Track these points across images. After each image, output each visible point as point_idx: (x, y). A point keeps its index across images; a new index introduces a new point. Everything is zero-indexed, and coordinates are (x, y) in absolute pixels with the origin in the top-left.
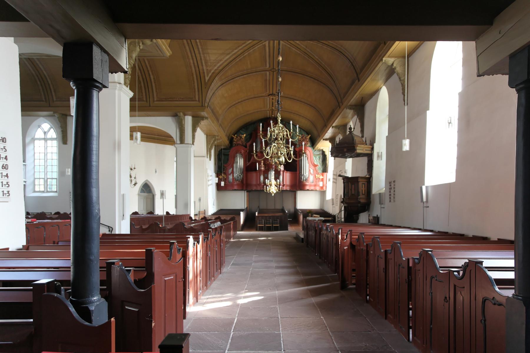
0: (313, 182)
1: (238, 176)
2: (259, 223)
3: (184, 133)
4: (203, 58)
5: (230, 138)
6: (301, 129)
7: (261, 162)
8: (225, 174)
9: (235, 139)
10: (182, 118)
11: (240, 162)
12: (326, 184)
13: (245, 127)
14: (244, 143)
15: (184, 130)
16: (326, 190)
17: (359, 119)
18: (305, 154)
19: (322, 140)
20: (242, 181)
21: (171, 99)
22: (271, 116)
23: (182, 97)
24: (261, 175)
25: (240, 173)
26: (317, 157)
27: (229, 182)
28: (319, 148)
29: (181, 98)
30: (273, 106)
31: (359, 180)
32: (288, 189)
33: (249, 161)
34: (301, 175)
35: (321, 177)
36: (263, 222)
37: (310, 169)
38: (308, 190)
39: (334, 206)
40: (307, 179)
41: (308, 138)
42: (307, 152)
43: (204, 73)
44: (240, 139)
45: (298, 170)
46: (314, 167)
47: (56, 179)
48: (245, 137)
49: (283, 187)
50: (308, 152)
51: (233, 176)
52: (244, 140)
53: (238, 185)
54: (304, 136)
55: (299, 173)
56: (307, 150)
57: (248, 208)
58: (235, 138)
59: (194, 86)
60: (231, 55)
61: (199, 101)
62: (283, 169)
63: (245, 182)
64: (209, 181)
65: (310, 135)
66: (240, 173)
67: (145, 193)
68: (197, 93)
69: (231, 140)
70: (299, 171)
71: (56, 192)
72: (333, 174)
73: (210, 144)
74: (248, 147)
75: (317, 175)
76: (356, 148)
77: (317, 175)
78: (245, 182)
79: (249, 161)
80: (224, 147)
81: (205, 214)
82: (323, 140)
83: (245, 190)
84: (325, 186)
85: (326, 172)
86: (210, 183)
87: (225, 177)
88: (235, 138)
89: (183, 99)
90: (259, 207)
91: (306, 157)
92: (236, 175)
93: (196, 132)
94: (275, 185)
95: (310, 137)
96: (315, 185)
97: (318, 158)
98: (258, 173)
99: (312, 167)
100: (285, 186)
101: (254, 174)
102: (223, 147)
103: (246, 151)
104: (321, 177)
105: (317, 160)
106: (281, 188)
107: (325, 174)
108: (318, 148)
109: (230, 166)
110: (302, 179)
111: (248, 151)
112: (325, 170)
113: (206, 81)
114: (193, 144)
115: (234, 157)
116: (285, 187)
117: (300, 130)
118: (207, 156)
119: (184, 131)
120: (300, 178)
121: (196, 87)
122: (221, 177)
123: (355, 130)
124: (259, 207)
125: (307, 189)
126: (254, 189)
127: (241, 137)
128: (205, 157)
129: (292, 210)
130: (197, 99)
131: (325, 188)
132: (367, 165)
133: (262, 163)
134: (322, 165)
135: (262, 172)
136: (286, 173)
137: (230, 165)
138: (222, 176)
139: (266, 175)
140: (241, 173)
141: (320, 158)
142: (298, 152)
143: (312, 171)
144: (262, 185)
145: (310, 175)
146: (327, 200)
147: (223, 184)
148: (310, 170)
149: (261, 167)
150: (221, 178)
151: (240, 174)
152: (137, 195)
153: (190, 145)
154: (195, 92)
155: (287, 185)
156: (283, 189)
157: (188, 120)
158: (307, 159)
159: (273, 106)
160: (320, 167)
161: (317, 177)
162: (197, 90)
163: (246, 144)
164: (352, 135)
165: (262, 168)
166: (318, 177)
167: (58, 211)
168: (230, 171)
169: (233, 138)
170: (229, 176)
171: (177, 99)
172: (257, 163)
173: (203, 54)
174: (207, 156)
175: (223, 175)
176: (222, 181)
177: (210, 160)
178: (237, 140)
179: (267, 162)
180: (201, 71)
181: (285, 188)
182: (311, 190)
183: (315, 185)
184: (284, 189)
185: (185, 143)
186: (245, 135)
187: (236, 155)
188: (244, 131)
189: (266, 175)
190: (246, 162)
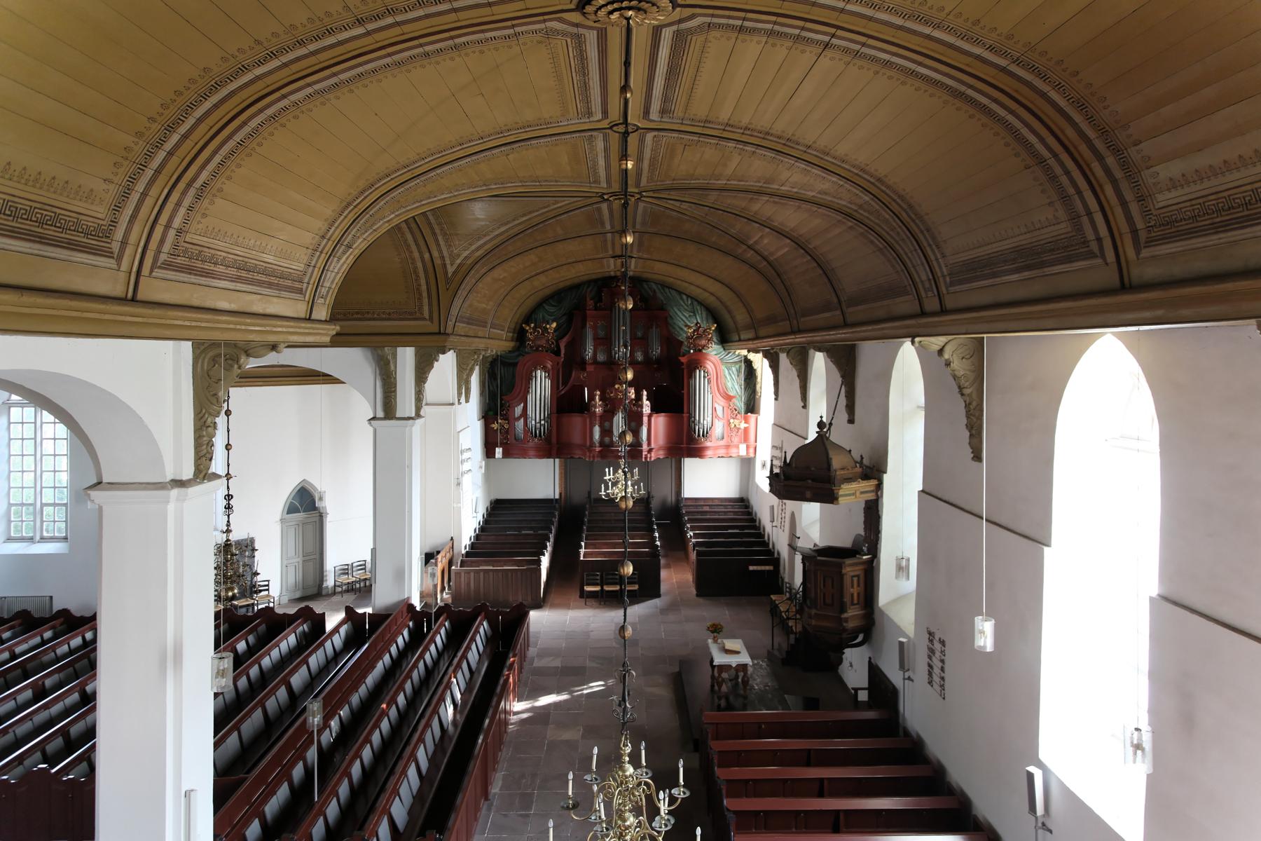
1: (538, 425)
2: (587, 579)
3: (395, 391)
4: (438, 231)
6: (693, 301)
7: (596, 395)
8: (505, 418)
9: (531, 335)
10: (390, 357)
11: (541, 387)
12: (756, 442)
13: (558, 296)
14: (553, 343)
15: (396, 384)
16: (755, 457)
17: (845, 386)
20: (548, 439)
21: (359, 316)
23: (387, 311)
24: (595, 426)
25: (542, 418)
26: (734, 369)
27: (515, 438)
29: (384, 313)
31: (844, 571)
32: (661, 457)
34: (694, 422)
35: (743, 425)
36: (599, 578)
37: (716, 405)
39: (774, 524)
42: (708, 366)
43: (443, 258)
44: (543, 334)
45: (685, 410)
46: (724, 401)
47: (65, 505)
48: (556, 330)
49: (649, 456)
50: (709, 366)
54: (700, 327)
55: (689, 418)
56: (708, 362)
59: (419, 285)
60: (511, 225)
61: (431, 319)
62: (649, 411)
63: (554, 440)
64: (462, 462)
67: (300, 512)
68: (425, 301)
69: (520, 336)
70: (689, 412)
71: (66, 538)
72: (773, 447)
73: (466, 369)
74: (563, 351)
75: (732, 421)
76: (838, 493)
77: (732, 421)
78: (554, 440)
79: (565, 384)
81: (453, 548)
84: (754, 446)
86: (466, 467)
89: (389, 314)
90: (589, 493)
91: (704, 377)
92: (533, 422)
93: (425, 383)
95: (716, 328)
96: (728, 447)
97: (735, 372)
100: (654, 450)
101: (576, 421)
104: (743, 425)
105: (733, 376)
106: (644, 456)
107: (752, 417)
109: (518, 398)
110: (695, 433)
112: (752, 406)
113: (450, 275)
114: (418, 415)
115: (529, 378)
116: (653, 454)
117: (692, 303)
118: (459, 400)
119: (395, 387)
120: (691, 430)
121: (424, 287)
122: (495, 426)
123: (832, 428)
124: (589, 493)
128: (453, 404)
129: (671, 499)
130: (426, 314)
132: (863, 511)
133: (597, 397)
134: (745, 389)
135: (598, 418)
137: (518, 395)
139: (607, 424)
140: (544, 419)
141: (739, 371)
142: (685, 364)
144: (598, 449)
145: (716, 421)
147: (499, 452)
148: (714, 409)
150: (495, 428)
151: (543, 422)
152: (279, 523)
153: (411, 421)
154: (420, 299)
156: (648, 460)
157: (406, 357)
158: (709, 383)
160: (740, 404)
161: (733, 426)
162: (425, 294)
163: (558, 346)
164: (824, 444)
166: (735, 425)
167: (66, 607)
168: (518, 410)
170: (516, 424)
171: (375, 316)
172: (586, 389)
173: (439, 224)
174: (459, 400)
175: (499, 421)
177: (467, 401)
178: (536, 338)
180: (438, 262)
181: (653, 456)
183: (728, 447)
184: (650, 458)
185: (398, 415)
186: (554, 325)
187: (534, 374)
188: (553, 306)
189: (607, 424)
190: (558, 388)
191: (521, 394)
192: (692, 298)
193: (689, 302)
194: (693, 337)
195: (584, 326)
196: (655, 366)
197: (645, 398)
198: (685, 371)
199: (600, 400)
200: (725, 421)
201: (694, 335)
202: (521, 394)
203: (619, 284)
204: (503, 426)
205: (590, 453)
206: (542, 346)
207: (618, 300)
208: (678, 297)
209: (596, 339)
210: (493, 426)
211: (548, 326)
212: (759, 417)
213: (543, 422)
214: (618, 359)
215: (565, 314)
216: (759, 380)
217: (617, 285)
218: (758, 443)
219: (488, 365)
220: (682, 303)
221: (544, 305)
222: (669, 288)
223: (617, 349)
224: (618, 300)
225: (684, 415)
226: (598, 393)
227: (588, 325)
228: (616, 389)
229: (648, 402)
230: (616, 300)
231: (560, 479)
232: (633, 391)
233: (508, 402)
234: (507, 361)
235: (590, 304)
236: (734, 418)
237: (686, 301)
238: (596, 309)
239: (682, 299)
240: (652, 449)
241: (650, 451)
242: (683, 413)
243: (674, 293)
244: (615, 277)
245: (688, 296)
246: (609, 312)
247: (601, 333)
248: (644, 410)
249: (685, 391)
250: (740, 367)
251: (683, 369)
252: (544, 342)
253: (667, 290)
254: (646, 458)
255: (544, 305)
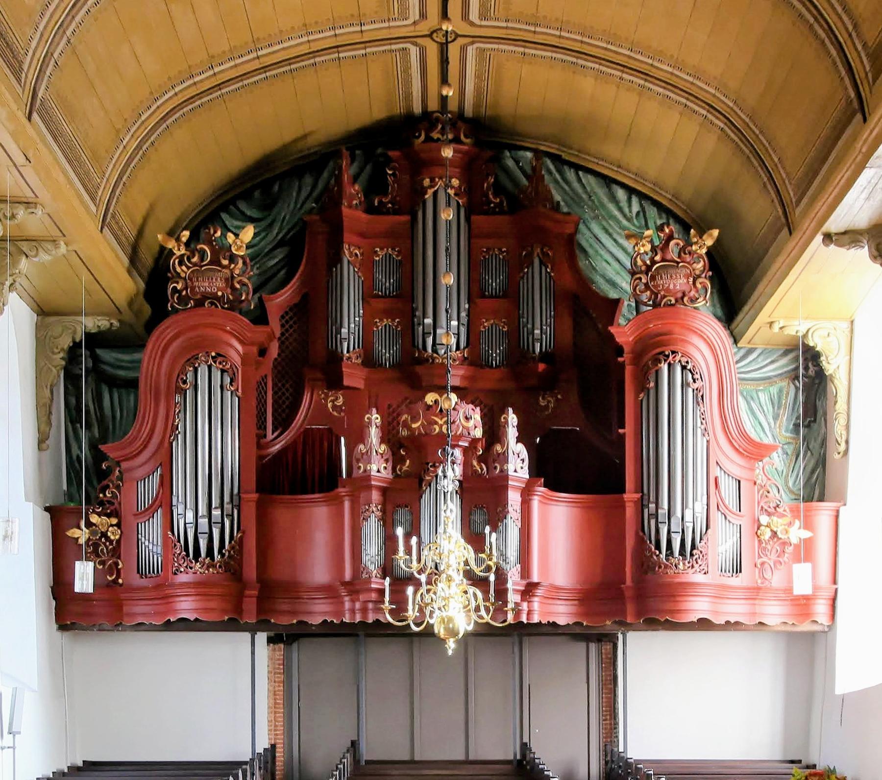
0: (738, 570)
5: (147, 258)
6: (647, 205)
12: (835, 581)
14: (243, 284)
18: (684, 368)
19: (819, 238)
22: (433, 105)
25: (215, 502)
26: (763, 397)
28: (776, 328)
30: (444, 80)
32: (562, 621)
33: (283, 423)
35: (797, 534)
37: (716, 472)
38: (704, 624)
40: (693, 547)
41: (704, 251)
44: (215, 261)
49: (525, 605)
51: (169, 524)
52: (243, 273)
53: (200, 587)
55: (641, 505)
57: (279, 754)
58: (183, 251)
62: (524, 474)
63: (250, 572)
65: (716, 233)
66: (215, 502)
70: (640, 488)
75: (764, 519)
77: (764, 519)
78: (250, 572)
80: (104, 323)
82: (828, 238)
83: (253, 630)
85: (821, 499)
87: (114, 535)
88: (183, 251)
91: (685, 385)
92: (190, 516)
94: (469, 575)
95: (718, 241)
96: (755, 593)
98: (347, 505)
99: (734, 464)
100: (539, 592)
102: (91, 323)
103: (263, 352)
104: (797, 534)
107: (823, 512)
108: (771, 324)
110: (658, 546)
111: (274, 350)
116: (536, 606)
124: (354, 745)
125: (694, 618)
126: (317, 620)
127: (221, 251)
131: (821, 609)
135: (375, 496)
136: (545, 500)
138: (89, 524)
141: (777, 404)
142: (626, 349)
143: (728, 488)
145: (717, 518)
146: (843, 698)
149: (367, 457)
155: (555, 593)
159: (444, 80)
161: (767, 534)
163: (261, 304)
165: (374, 467)
166: (774, 534)
169: (171, 253)
176: (80, 559)
179: (406, 425)
182: (728, 626)
183: (755, 593)
184: (529, 613)
186: (248, 233)
187: (190, 376)
190: (262, 426)
191: (155, 440)
192: (642, 196)
193: (636, 207)
194: (649, 268)
195: (336, 259)
196: (541, 367)
197: (512, 433)
198: (628, 370)
199: (383, 440)
200: (745, 522)
201: (653, 262)
202: (155, 440)
203: (435, 135)
204: (104, 535)
205: (353, 601)
206: (214, 297)
207: (432, 180)
208: (601, 192)
209: (368, 296)
210: (74, 533)
211: (231, 237)
212: (842, 510)
213: (216, 513)
214: (435, 351)
215: (280, 244)
216: (841, 406)
217: (429, 139)
218: (840, 585)
219: (59, 359)
220: (616, 213)
221: (224, 216)
222: (577, 168)
223: (429, 321)
224: (432, 180)
225: (625, 496)
226: (375, 417)
227: (346, 257)
228: (429, 407)
229: (521, 448)
230: (427, 182)
231: (273, 708)
232: (477, 416)
233: (118, 464)
234: (122, 373)
235: (354, 191)
236: (769, 514)
237: (624, 204)
238: (370, 209)
239: (614, 199)
240: (536, 585)
241: (528, 591)
242: (623, 491)
243: (590, 181)
244: (426, 114)
245: (631, 191)
246: (405, 218)
247: (385, 282)
248: (510, 467)
249: (628, 431)
250: (780, 391)
251: (622, 366)
252: (220, 284)
253: (570, 174)
254: (517, 612)
255: (224, 216)
